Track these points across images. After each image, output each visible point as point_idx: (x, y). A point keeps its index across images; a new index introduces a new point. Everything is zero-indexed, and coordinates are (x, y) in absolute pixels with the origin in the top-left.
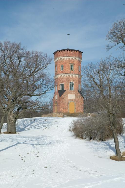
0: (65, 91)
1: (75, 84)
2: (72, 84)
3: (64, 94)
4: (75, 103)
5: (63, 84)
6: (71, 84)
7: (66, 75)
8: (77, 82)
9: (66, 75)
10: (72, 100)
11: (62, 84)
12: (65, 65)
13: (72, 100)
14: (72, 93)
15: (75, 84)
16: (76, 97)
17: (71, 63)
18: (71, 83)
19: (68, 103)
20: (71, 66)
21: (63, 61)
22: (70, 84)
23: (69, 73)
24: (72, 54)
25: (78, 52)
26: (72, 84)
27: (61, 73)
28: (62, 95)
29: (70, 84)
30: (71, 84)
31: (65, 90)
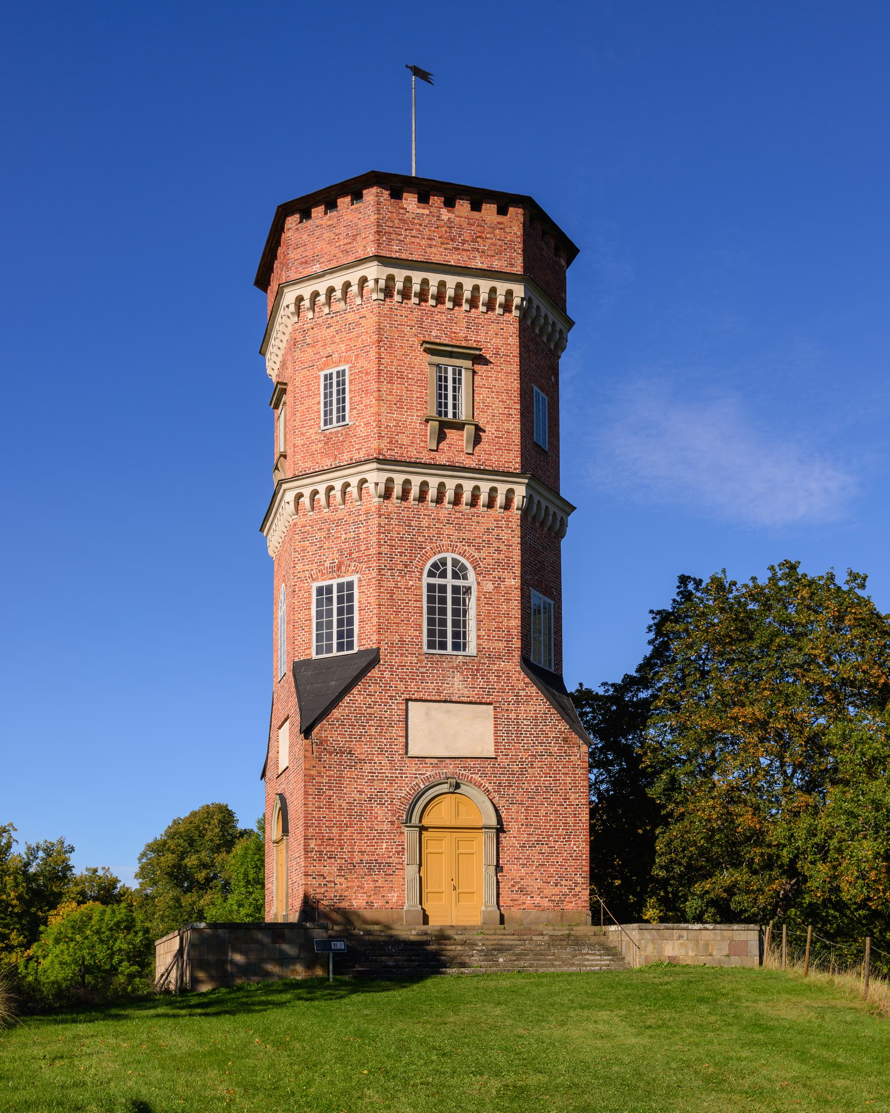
2: (449, 582)
5: (350, 585)
6: (443, 588)
8: (508, 567)
11: (335, 582)
12: (362, 363)
13: (450, 769)
14: (457, 685)
15: (489, 587)
16: (505, 732)
17: (434, 335)
18: (438, 569)
20: (442, 379)
21: (351, 317)
22: (426, 580)
23: (413, 454)
25: (516, 214)
26: (456, 589)
27: (327, 463)
29: (426, 580)
30: (443, 588)
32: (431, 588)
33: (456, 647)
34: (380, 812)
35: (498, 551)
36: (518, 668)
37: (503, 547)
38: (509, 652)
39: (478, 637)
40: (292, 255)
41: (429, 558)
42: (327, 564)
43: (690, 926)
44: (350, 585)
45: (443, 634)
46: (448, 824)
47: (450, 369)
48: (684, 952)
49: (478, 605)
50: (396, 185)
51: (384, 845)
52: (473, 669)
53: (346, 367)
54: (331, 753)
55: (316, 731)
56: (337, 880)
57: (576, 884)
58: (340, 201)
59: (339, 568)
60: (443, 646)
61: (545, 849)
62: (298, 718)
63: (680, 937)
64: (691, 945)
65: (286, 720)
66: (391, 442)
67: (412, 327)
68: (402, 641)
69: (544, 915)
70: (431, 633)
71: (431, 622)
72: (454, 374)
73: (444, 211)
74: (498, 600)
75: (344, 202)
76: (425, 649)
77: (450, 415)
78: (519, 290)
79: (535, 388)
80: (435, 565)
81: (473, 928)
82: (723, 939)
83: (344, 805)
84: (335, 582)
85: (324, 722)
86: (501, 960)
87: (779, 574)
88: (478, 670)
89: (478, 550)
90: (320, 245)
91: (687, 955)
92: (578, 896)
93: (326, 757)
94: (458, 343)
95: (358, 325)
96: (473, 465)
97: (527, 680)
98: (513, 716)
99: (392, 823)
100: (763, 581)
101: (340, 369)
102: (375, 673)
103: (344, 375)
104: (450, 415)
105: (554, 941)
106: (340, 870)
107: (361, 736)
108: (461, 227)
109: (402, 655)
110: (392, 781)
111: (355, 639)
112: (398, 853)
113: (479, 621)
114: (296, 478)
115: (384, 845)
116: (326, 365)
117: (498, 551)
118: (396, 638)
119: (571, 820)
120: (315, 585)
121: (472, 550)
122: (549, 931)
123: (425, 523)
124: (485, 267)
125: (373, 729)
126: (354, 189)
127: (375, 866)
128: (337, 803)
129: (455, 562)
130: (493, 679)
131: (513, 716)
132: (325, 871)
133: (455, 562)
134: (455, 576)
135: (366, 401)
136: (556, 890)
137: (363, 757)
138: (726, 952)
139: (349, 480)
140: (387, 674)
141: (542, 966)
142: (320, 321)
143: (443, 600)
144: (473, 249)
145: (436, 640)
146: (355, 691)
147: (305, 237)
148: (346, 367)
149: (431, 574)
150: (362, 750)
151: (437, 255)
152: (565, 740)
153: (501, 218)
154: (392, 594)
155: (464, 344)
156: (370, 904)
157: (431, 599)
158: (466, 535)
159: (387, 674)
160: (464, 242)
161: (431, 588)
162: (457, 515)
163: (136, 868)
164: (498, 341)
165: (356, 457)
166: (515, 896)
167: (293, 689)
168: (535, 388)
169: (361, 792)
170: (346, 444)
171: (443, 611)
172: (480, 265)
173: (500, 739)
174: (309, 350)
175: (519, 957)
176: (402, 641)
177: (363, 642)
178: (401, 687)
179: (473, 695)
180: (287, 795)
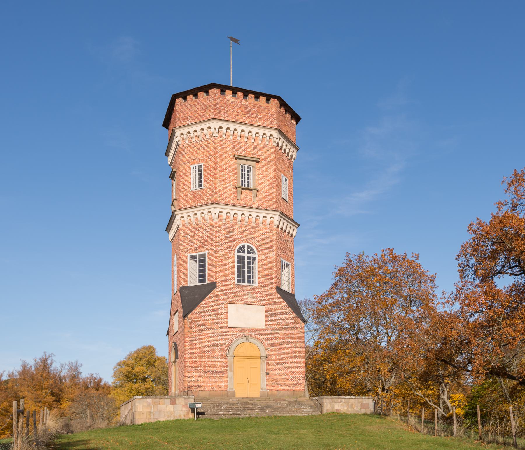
0: (213, 289)
1: (263, 257)
2: (246, 255)
3: (206, 303)
4: (262, 348)
5: (204, 255)
6: (243, 258)
7: (215, 210)
8: (271, 249)
9: (217, 211)
10: (248, 333)
11: (197, 254)
12: (209, 163)
14: (250, 297)
15: (263, 257)
16: (269, 317)
17: (239, 152)
18: (241, 249)
19: (229, 346)
21: (204, 143)
22: (236, 254)
23: (231, 201)
24: (246, 111)
25: (274, 102)
26: (249, 258)
27: (194, 204)
28: (198, 309)
29: (236, 254)
30: (243, 258)
31: (213, 286)
32: (238, 257)
33: (249, 282)
34: (217, 350)
35: (267, 242)
36: (275, 291)
37: (269, 241)
38: (271, 285)
39: (259, 278)
40: (178, 116)
41: (237, 245)
42: (194, 246)
43: (345, 397)
44: (204, 255)
45: (244, 276)
46: (246, 355)
47: (246, 167)
48: (342, 408)
49: (258, 265)
50: (223, 89)
51: (219, 364)
52: (257, 292)
53: (202, 164)
54: (196, 326)
55: (189, 316)
56: (199, 378)
57: (300, 380)
58: (199, 94)
59: (199, 248)
60: (244, 281)
61: (287, 366)
62: (182, 310)
63: (341, 402)
64: (345, 405)
65: (177, 311)
66: (221, 196)
67: (230, 148)
68: (226, 279)
69: (286, 392)
70: (238, 276)
71: (238, 271)
72: (248, 168)
73: (243, 101)
74: (267, 263)
75: (201, 94)
76: (236, 282)
77: (246, 186)
78: (276, 134)
79: (282, 175)
80: (240, 248)
81: (256, 398)
82: (358, 402)
83: (202, 347)
84: (197, 254)
85: (193, 312)
86: (267, 411)
87: (385, 253)
88: (258, 292)
89: (258, 242)
90: (190, 112)
91: (344, 409)
92: (301, 386)
93: (193, 327)
94: (249, 156)
95: (207, 147)
96: (256, 207)
97: (279, 296)
98: (273, 311)
99: (222, 355)
100: (379, 256)
101: (199, 165)
102: (214, 292)
103: (201, 167)
104: (246, 186)
105: (290, 403)
106: (200, 374)
107: (209, 318)
108: (250, 108)
109: (226, 285)
110: (222, 337)
111: (206, 278)
112: (225, 367)
113: (259, 272)
114: (180, 209)
115: (219, 364)
116: (193, 163)
117: (267, 242)
118: (224, 278)
119: (297, 354)
120: (189, 255)
121: (255, 242)
122: (288, 399)
123: (236, 230)
124: (261, 124)
125: (214, 316)
126: (206, 89)
127: (215, 373)
128: (198, 346)
129: (249, 247)
130: (265, 295)
131: (273, 311)
132: (194, 374)
133: (249, 247)
134: (249, 252)
135: (210, 179)
136: (291, 383)
137: (210, 327)
138: (360, 408)
139: (203, 211)
140: (220, 293)
141: (285, 413)
142: (191, 144)
143: (244, 263)
144: (256, 117)
145: (241, 279)
146: (206, 300)
147: (184, 109)
148: (202, 164)
149: (238, 252)
150: (209, 324)
151: (240, 119)
152: (295, 321)
153: (267, 105)
154: (222, 259)
155: (252, 156)
156: (213, 388)
157: (238, 262)
158: (253, 236)
159: (220, 293)
160: (252, 114)
161: (238, 257)
162: (250, 227)
163: (112, 373)
164: (267, 156)
165: (206, 202)
166: (273, 385)
167: (180, 299)
168: (282, 175)
169: (209, 342)
170: (202, 196)
171: (244, 267)
172: (259, 124)
173: (268, 320)
174: (186, 156)
175: (275, 410)
176: (226, 279)
177: (210, 279)
178: (226, 298)
179: (256, 302)
180: (177, 343)
